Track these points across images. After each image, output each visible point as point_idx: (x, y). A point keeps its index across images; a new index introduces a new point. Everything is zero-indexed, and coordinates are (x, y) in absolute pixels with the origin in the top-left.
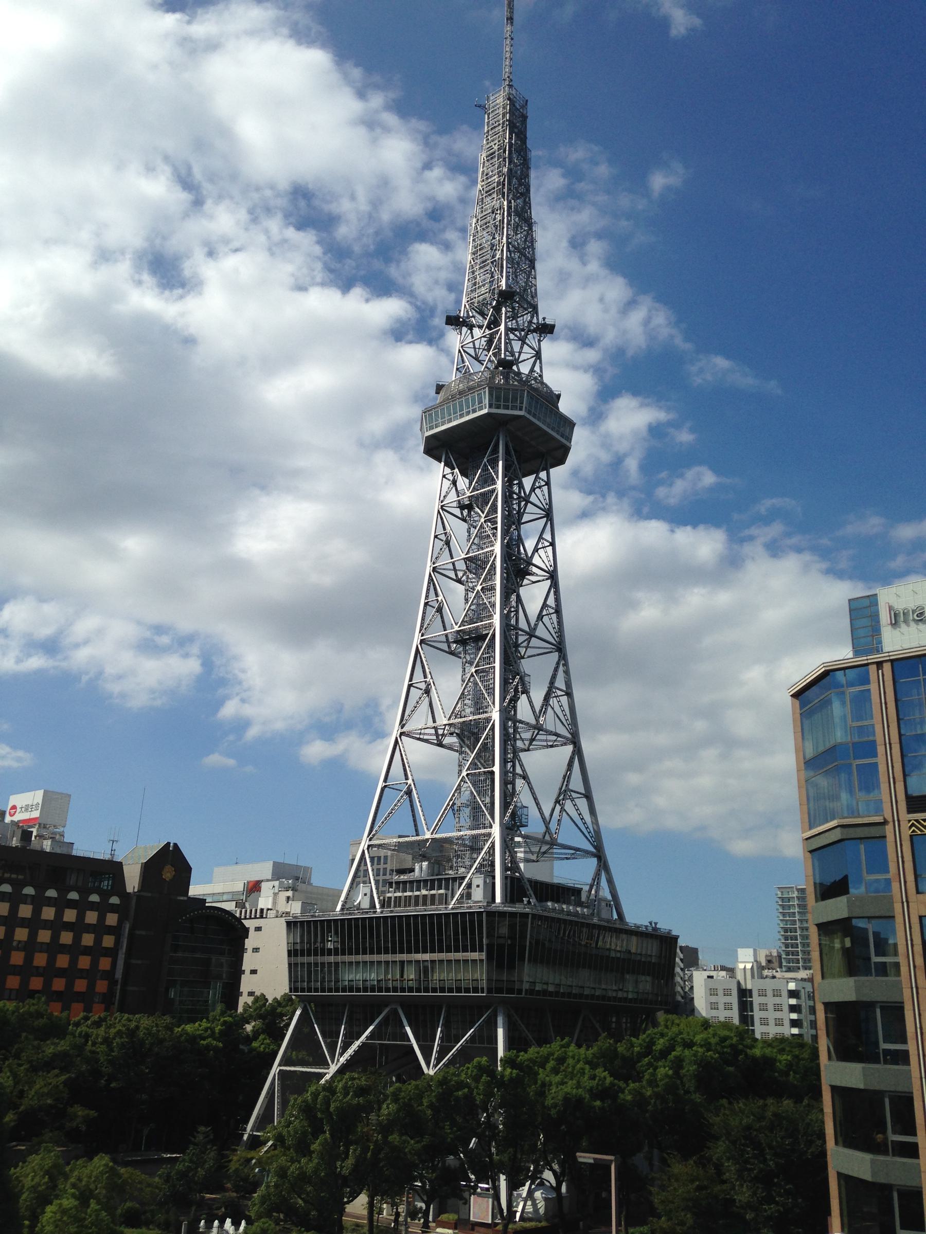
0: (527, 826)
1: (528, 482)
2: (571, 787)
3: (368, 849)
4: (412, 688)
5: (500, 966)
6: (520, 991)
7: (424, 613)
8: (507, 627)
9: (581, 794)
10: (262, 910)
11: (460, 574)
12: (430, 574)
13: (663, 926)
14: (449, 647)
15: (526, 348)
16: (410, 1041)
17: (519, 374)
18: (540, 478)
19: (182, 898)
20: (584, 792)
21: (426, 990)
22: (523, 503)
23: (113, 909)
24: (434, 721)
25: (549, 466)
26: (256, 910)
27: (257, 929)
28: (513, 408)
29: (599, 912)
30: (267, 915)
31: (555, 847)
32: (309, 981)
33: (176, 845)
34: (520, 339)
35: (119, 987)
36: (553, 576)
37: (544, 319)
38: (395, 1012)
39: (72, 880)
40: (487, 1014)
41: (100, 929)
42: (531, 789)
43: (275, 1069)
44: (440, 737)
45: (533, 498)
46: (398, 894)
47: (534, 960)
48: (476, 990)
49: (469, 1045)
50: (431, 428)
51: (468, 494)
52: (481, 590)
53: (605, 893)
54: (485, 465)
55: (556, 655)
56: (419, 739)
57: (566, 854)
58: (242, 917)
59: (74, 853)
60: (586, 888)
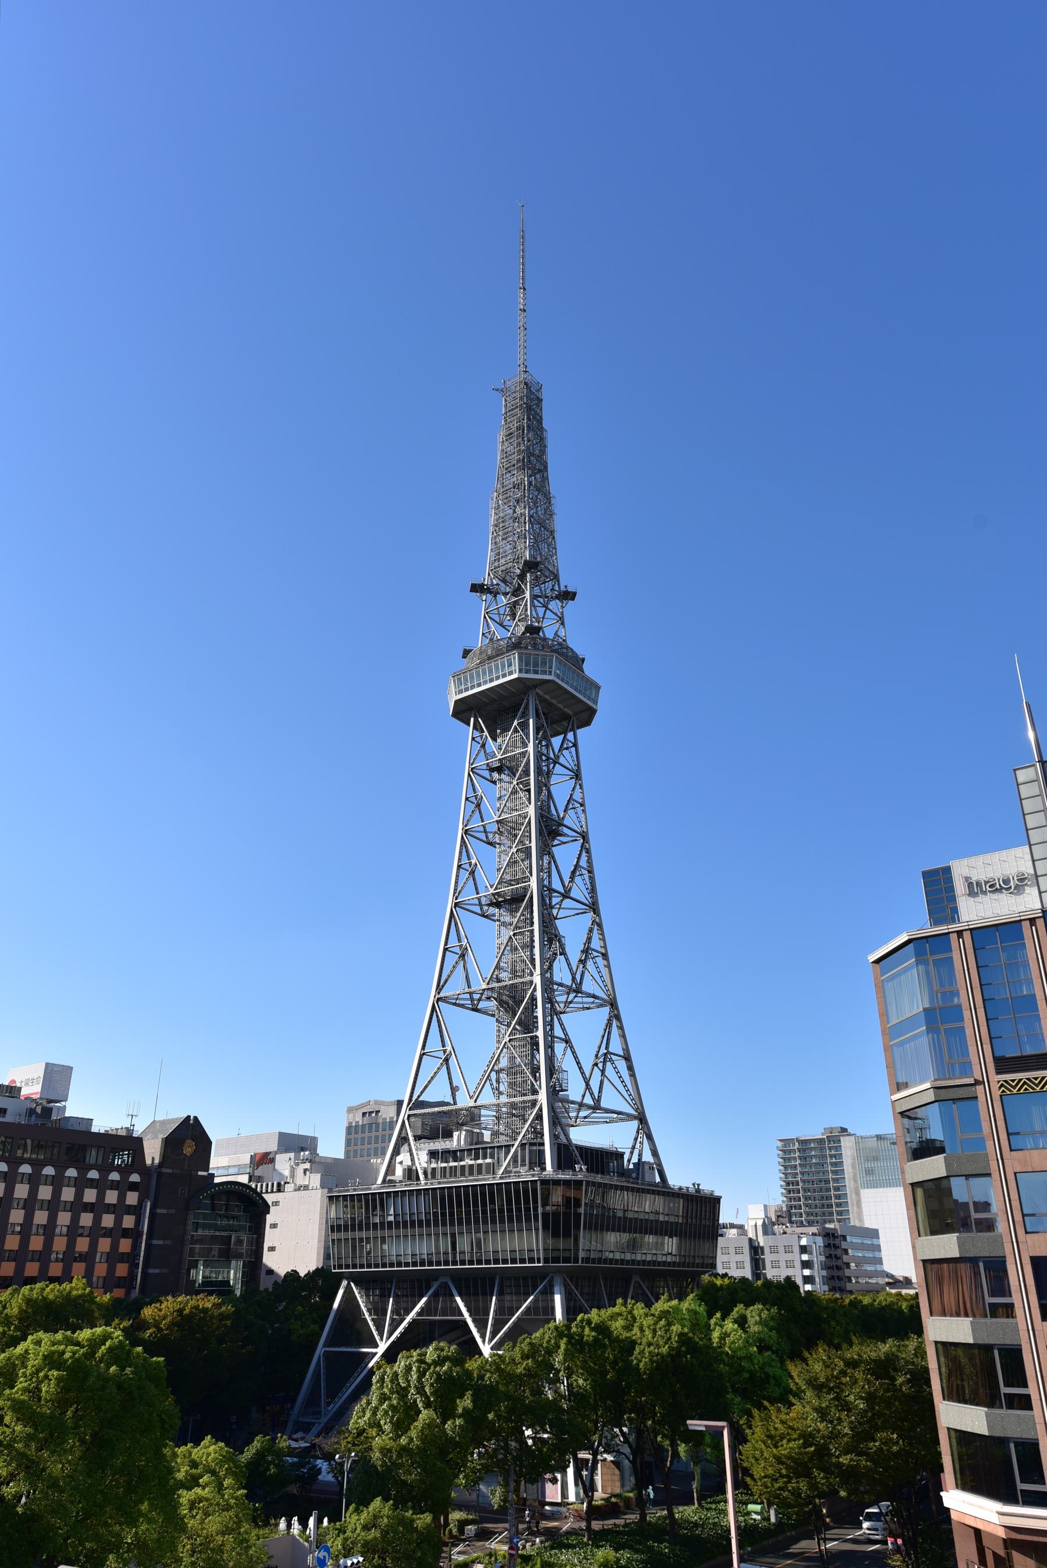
1: (556, 741)
2: (611, 1050)
3: (408, 1119)
4: (447, 952)
5: (556, 1235)
6: (576, 1261)
7: (457, 876)
8: (546, 890)
9: (620, 1056)
11: (490, 836)
12: (462, 837)
13: (706, 1187)
14: (481, 909)
15: (549, 614)
16: (463, 1316)
17: (545, 639)
18: (568, 740)
19: (200, 1173)
20: (623, 1054)
21: (479, 1262)
22: (552, 766)
23: (133, 1187)
24: (469, 987)
27: (274, 1204)
28: (544, 672)
31: (598, 1111)
32: (354, 1257)
33: (196, 1118)
34: (544, 606)
35: (140, 1270)
37: (566, 587)
38: (445, 1286)
39: (92, 1156)
41: (119, 1209)
42: (574, 1052)
43: (320, 1350)
44: (476, 1002)
45: (562, 760)
46: (444, 1165)
47: (589, 1227)
48: (532, 1260)
49: (524, 1317)
50: (461, 692)
51: (499, 757)
53: (648, 1157)
56: (455, 1004)
57: (606, 1118)
58: (264, 1191)
59: (95, 1129)
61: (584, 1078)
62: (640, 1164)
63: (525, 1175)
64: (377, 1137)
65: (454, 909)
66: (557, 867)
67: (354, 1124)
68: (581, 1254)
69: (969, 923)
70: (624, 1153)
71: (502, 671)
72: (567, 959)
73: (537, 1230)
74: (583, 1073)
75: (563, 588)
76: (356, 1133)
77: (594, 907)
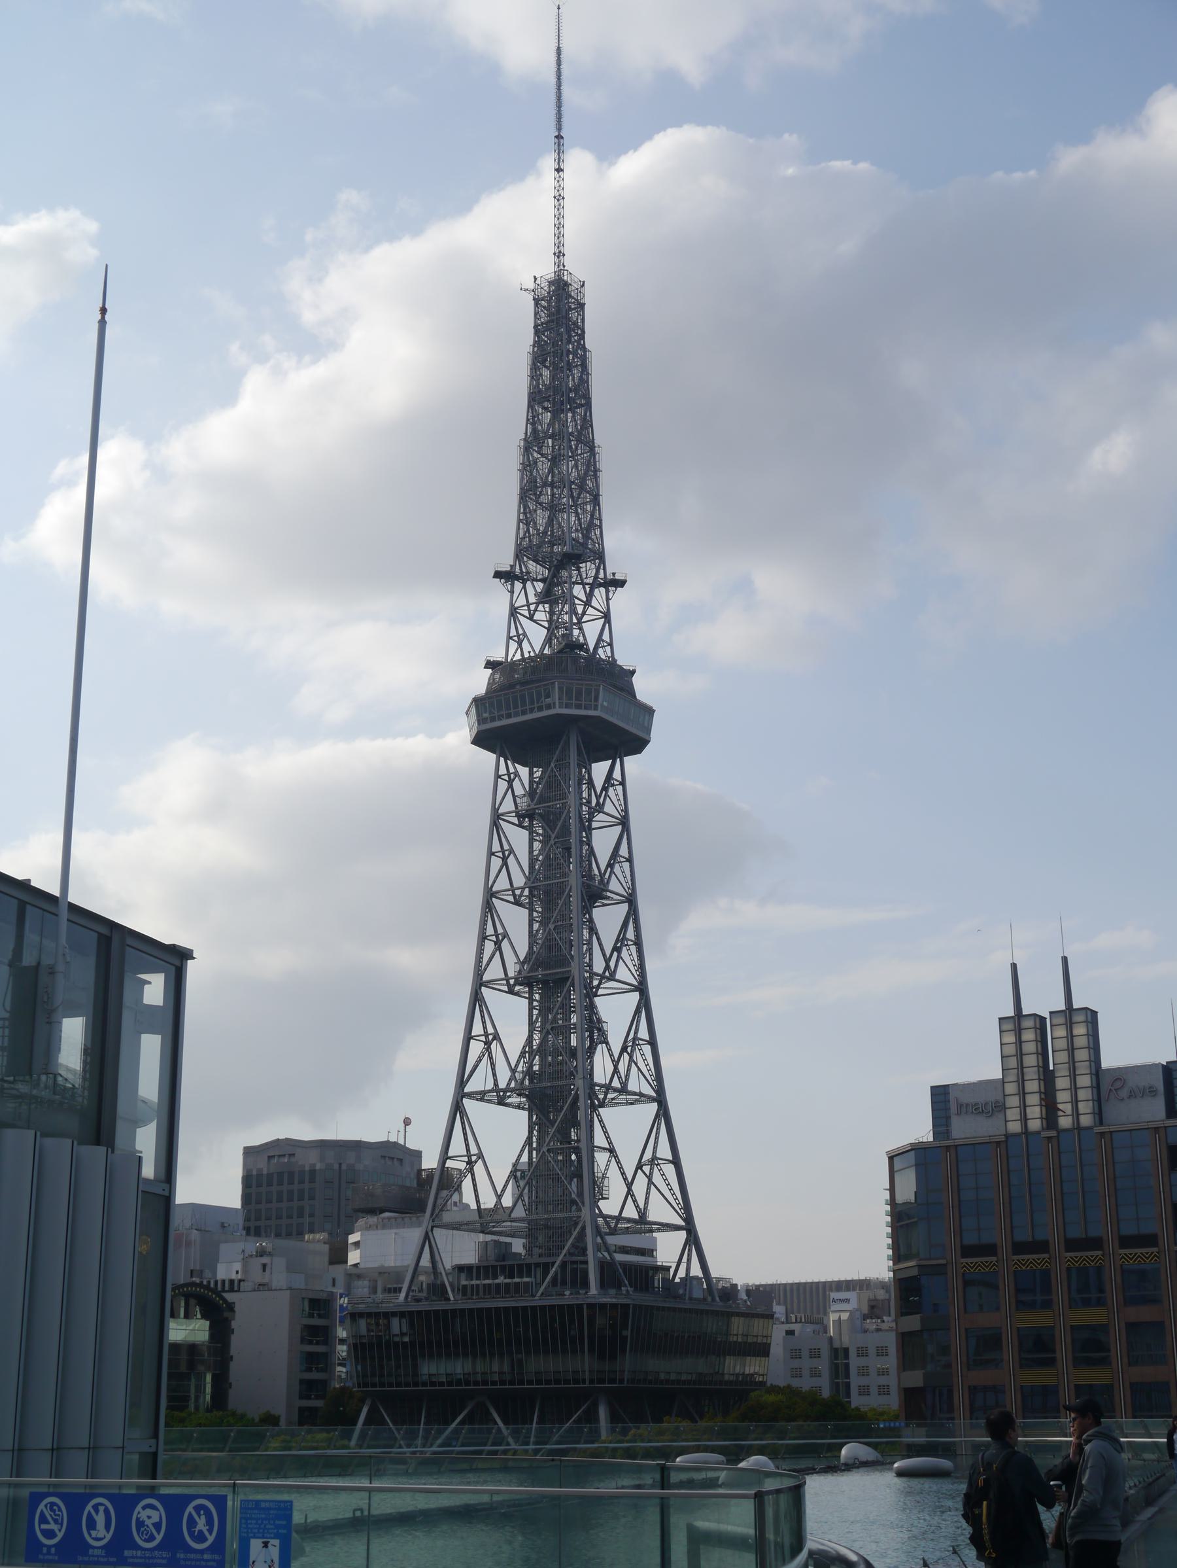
0: (608, 1198)
2: (658, 1155)
6: (622, 1381)
10: (232, 1282)
15: (590, 611)
21: (521, 1382)
26: (216, 1282)
36: (631, 900)
37: (614, 574)
40: (586, 1405)
42: (618, 1162)
48: (576, 1381)
52: (554, 929)
53: (696, 1271)
54: (552, 770)
55: (636, 996)
60: (674, 1266)
61: (633, 1196)
62: (688, 1279)
63: (568, 1297)
64: (291, 1192)
65: (479, 991)
67: (255, 1173)
68: (626, 1376)
70: (671, 1267)
71: (538, 703)
72: (609, 1050)
73: (583, 1352)
74: (625, 1179)
75: (609, 577)
76: (259, 1185)
77: (641, 988)
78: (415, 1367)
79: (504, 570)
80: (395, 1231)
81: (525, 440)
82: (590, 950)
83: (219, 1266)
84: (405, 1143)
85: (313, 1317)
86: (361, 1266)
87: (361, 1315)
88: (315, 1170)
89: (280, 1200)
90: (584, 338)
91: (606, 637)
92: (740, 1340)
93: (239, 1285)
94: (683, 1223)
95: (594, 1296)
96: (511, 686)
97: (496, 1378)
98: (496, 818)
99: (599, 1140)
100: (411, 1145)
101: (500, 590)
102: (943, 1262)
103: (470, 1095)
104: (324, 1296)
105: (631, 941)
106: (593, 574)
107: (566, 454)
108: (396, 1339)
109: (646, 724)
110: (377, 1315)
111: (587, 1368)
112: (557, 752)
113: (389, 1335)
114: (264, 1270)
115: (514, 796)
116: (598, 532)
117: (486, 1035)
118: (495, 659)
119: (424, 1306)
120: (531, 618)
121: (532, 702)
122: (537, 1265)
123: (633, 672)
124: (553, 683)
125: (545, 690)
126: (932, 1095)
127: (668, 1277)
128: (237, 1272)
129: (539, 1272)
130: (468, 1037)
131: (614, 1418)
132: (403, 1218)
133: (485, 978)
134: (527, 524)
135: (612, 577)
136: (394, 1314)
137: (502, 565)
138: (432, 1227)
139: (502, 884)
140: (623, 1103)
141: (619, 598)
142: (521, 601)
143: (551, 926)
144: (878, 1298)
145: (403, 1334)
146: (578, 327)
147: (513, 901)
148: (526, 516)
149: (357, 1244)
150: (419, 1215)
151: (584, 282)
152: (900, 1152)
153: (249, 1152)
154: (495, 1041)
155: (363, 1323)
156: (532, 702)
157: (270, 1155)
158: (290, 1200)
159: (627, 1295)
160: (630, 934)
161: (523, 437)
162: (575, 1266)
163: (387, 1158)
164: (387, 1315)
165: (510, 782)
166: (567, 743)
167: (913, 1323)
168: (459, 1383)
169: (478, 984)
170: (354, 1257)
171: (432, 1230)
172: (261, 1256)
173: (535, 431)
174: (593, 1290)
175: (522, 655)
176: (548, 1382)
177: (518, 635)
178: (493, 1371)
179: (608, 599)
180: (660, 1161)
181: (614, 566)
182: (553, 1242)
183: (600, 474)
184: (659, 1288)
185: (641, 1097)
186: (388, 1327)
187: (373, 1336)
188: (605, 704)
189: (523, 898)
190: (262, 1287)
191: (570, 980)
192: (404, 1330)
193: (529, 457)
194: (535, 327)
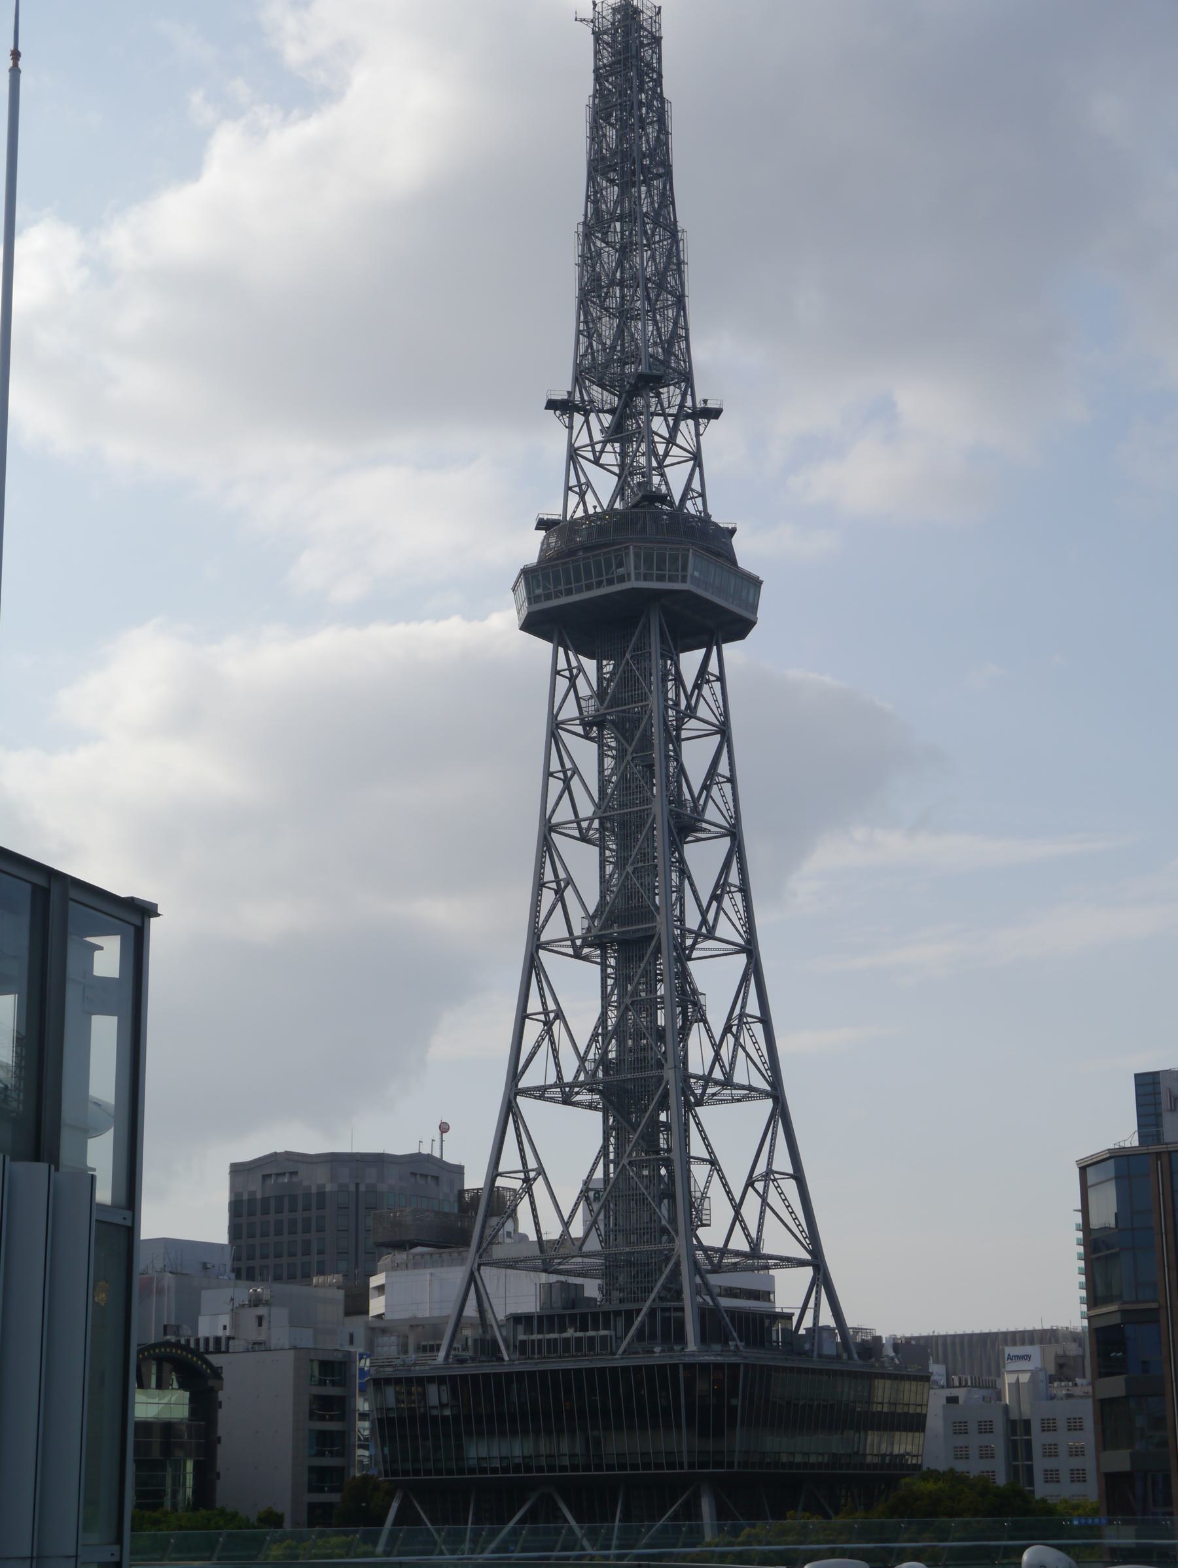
0: (709, 1225)
2: (775, 1168)
6: (731, 1465)
10: (218, 1340)
15: (675, 451)
21: (599, 1467)
25: (720, 642)
26: (197, 1341)
29: (820, 1346)
30: (228, 1348)
36: (734, 832)
37: (705, 401)
40: (683, 1498)
42: (722, 1178)
48: (671, 1465)
52: (634, 872)
53: (827, 1319)
54: (627, 663)
55: (742, 959)
60: (797, 1313)
61: (742, 1221)
62: (816, 1330)
63: (659, 1355)
64: (293, 1223)
65: (535, 955)
66: (692, 885)
67: (245, 1197)
69: (1168, 1146)
70: (793, 1314)
71: (607, 574)
72: (708, 1030)
73: (679, 1426)
74: (732, 1200)
75: (700, 405)
76: (252, 1213)
77: (750, 948)
78: (460, 1448)
79: (559, 398)
80: (431, 1270)
81: (585, 224)
82: (681, 899)
83: (201, 1319)
84: (442, 1156)
85: (325, 1384)
86: (387, 1317)
87: (388, 1381)
88: (324, 1193)
89: (279, 1232)
90: (662, 85)
91: (696, 485)
92: (885, 1410)
93: (227, 1344)
94: (808, 1257)
95: (692, 1354)
96: (572, 553)
97: (566, 1461)
98: (555, 727)
99: (697, 1148)
100: (450, 1158)
101: (554, 423)
102: (1154, 1305)
103: (526, 1092)
104: (339, 1357)
105: (735, 886)
106: (678, 402)
107: (639, 241)
108: (435, 1412)
109: (751, 600)
110: (409, 1381)
111: (684, 1448)
112: (634, 639)
113: (425, 1407)
114: (260, 1324)
115: (578, 698)
116: (683, 345)
117: (546, 1012)
118: (550, 517)
119: (470, 1369)
120: (596, 462)
121: (600, 574)
122: (618, 1313)
123: (732, 532)
124: (627, 548)
125: (616, 559)
126: (1137, 1085)
127: (790, 1328)
128: (225, 1327)
129: (620, 1323)
130: (523, 1016)
131: (721, 1513)
132: (440, 1254)
133: (543, 938)
134: (590, 337)
135: (702, 406)
136: (431, 1379)
137: (556, 393)
138: (479, 1265)
139: (564, 813)
140: (727, 1100)
141: (713, 431)
142: (583, 439)
143: (629, 869)
144: (1068, 1353)
145: (443, 1406)
146: (653, 70)
147: (578, 836)
148: (588, 326)
149: (381, 1289)
150: (461, 1249)
151: (660, 8)
152: (1095, 1160)
153: (237, 1170)
154: (558, 1021)
155: (390, 1392)
156: (600, 574)
157: (264, 1173)
158: (292, 1232)
159: (736, 1352)
160: (734, 878)
161: (582, 219)
162: (667, 1314)
163: (418, 1176)
164: (422, 1381)
165: (572, 680)
166: (647, 628)
167: (1115, 1386)
168: (517, 1468)
169: (535, 946)
170: (377, 1305)
171: (479, 1270)
172: (256, 1306)
173: (597, 212)
174: (692, 1346)
175: (586, 510)
176: (634, 1467)
177: (580, 485)
178: (561, 1452)
179: (698, 435)
180: (777, 1176)
181: (705, 392)
182: (638, 1282)
183: (685, 268)
184: (778, 1342)
185: (752, 1092)
186: (424, 1395)
187: (404, 1408)
188: (696, 574)
189: (591, 832)
190: (258, 1346)
191: (655, 939)
192: (445, 1400)
193: (590, 246)
194: (596, 70)
